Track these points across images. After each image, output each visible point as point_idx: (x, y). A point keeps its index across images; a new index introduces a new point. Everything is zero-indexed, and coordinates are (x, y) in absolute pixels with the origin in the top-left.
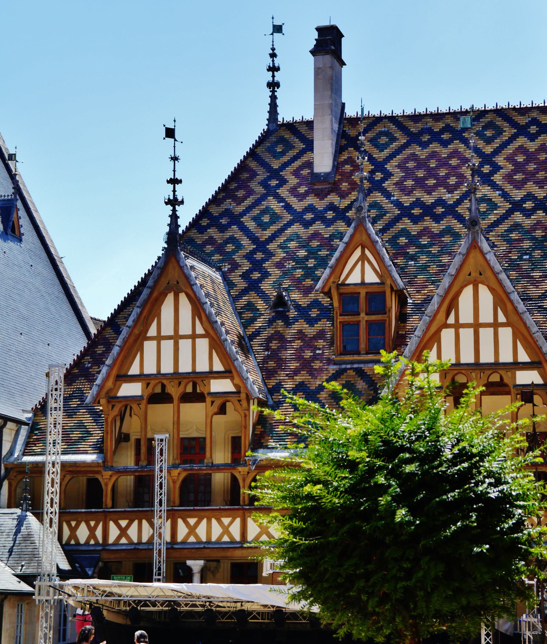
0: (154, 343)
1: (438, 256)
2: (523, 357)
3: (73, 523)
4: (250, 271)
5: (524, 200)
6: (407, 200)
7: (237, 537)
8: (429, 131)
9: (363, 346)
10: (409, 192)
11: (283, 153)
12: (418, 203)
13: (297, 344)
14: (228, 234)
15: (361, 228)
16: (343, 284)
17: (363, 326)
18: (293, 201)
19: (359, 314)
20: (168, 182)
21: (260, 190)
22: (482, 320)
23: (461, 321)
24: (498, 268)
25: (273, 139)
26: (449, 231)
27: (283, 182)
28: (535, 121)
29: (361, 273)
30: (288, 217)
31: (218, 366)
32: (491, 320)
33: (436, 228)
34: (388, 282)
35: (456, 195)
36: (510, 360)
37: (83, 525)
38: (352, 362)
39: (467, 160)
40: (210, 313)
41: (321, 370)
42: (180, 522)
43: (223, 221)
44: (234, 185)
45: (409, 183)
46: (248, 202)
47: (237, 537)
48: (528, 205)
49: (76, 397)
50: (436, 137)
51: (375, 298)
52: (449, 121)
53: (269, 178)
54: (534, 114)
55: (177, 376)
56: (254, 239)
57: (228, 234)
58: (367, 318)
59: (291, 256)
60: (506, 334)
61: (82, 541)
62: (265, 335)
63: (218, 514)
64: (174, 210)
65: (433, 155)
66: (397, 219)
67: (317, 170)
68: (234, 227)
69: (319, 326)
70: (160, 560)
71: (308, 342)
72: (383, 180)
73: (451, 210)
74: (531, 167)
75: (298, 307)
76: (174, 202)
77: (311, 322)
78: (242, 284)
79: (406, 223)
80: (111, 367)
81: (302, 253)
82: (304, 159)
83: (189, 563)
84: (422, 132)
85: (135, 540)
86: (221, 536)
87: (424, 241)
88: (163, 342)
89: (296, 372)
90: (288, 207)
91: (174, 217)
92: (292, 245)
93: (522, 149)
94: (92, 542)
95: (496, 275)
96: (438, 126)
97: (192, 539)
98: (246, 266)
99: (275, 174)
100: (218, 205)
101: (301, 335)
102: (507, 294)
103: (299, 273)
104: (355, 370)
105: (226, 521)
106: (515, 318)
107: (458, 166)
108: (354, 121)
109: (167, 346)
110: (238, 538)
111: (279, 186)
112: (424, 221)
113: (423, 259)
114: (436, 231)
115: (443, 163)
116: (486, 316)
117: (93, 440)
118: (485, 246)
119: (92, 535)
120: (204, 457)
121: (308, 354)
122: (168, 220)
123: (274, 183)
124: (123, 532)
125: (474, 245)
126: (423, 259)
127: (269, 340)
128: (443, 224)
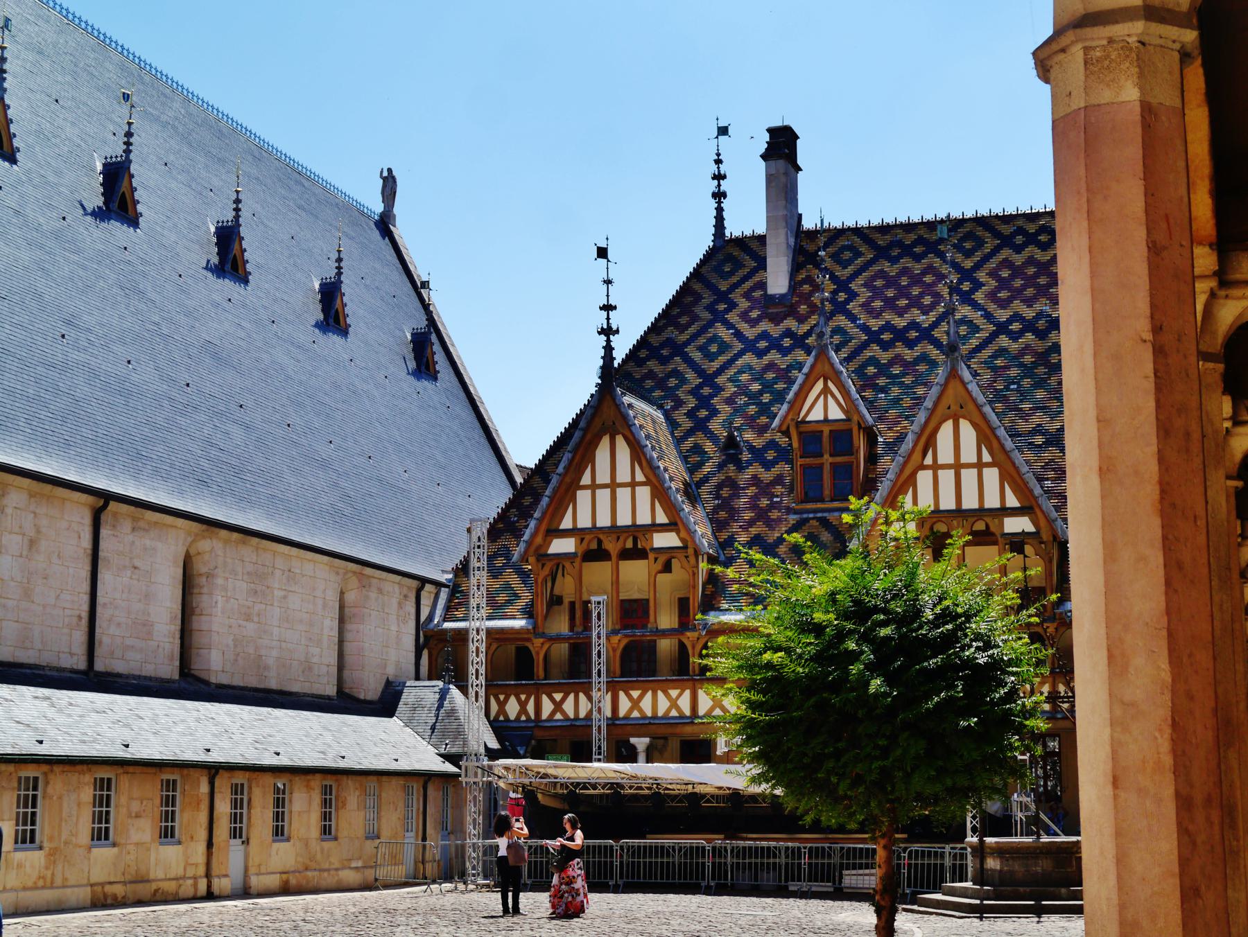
1: (912, 388)
2: (1012, 501)
3: (502, 697)
4: (696, 409)
5: (1010, 321)
6: (875, 324)
7: (687, 712)
8: (899, 243)
9: (827, 492)
10: (877, 315)
11: (731, 273)
12: (888, 327)
13: (751, 491)
14: (671, 367)
16: (803, 422)
17: (827, 468)
18: (743, 327)
19: (822, 456)
20: (601, 308)
21: (706, 315)
22: (963, 460)
23: (940, 462)
24: (981, 399)
25: (720, 256)
26: (924, 358)
27: (732, 306)
28: (1021, 231)
29: (824, 408)
30: (739, 346)
31: (662, 518)
33: (908, 354)
34: (855, 418)
35: (932, 317)
36: (997, 505)
37: (513, 699)
38: (815, 511)
39: (943, 277)
40: (652, 458)
41: (779, 520)
42: (622, 695)
43: (665, 352)
44: (676, 311)
45: (878, 304)
46: (692, 329)
47: (687, 712)
48: (1015, 326)
49: (501, 556)
50: (907, 251)
51: (840, 436)
52: (922, 232)
53: (716, 302)
54: (1020, 223)
55: (614, 529)
56: (700, 372)
57: (671, 367)
58: (831, 460)
61: (512, 717)
62: (714, 481)
63: (665, 686)
64: (608, 341)
65: (905, 271)
66: (864, 346)
68: (677, 359)
69: (776, 470)
70: (599, 738)
71: (765, 489)
72: (847, 301)
73: (926, 334)
74: (1018, 283)
75: (752, 449)
76: (608, 332)
77: (768, 465)
78: (687, 424)
79: (875, 350)
80: (540, 520)
81: (756, 387)
82: (756, 279)
83: (633, 740)
84: (892, 245)
85: (572, 716)
86: (669, 710)
87: (896, 370)
88: (598, 492)
89: (751, 523)
90: (738, 335)
91: (609, 349)
92: (744, 377)
93: (1006, 263)
94: (523, 718)
95: (979, 407)
96: (909, 239)
97: (635, 714)
98: (692, 403)
99: (723, 297)
100: (659, 334)
101: (755, 480)
102: (993, 430)
103: (752, 409)
104: (819, 519)
105: (674, 693)
106: (1001, 457)
107: (934, 284)
108: (813, 234)
109: (603, 496)
110: (687, 712)
111: (727, 311)
112: (895, 347)
113: (895, 391)
114: (908, 358)
115: (916, 280)
116: (969, 455)
117: (521, 603)
118: (966, 375)
119: (523, 710)
120: (648, 622)
121: (764, 502)
122: (602, 353)
123: (722, 307)
124: (558, 706)
125: (953, 374)
126: (895, 391)
127: (719, 487)
128: (918, 351)
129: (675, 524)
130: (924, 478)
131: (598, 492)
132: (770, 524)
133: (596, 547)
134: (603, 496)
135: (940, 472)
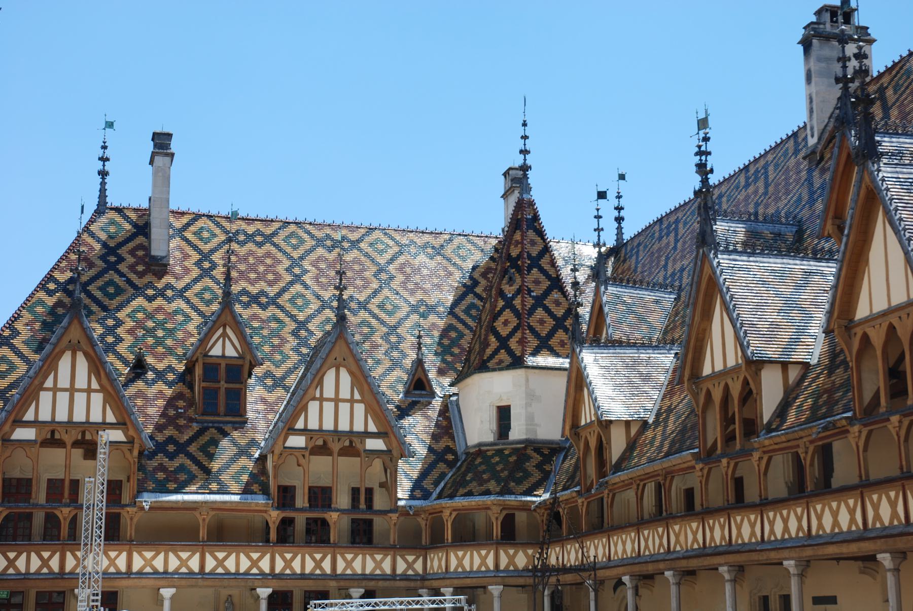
0: (51, 393)
2: (372, 428)
9: (222, 409)
12: (244, 292)
15: (227, 310)
22: (341, 397)
23: (325, 396)
25: (103, 220)
27: (121, 259)
28: (328, 237)
32: (349, 397)
33: (264, 314)
34: (248, 357)
36: (362, 429)
38: (213, 422)
39: (280, 262)
41: (187, 427)
47: (123, 569)
55: (70, 424)
58: (226, 385)
59: (140, 324)
60: (360, 409)
67: (153, 253)
73: (273, 302)
84: (237, 232)
87: (256, 324)
88: (59, 394)
92: (140, 315)
96: (251, 229)
109: (63, 398)
116: (345, 393)
120: (30, 498)
129: (125, 424)
130: (313, 407)
131: (59, 394)
132: (179, 428)
133: (52, 435)
134: (63, 398)
135: (325, 403)
